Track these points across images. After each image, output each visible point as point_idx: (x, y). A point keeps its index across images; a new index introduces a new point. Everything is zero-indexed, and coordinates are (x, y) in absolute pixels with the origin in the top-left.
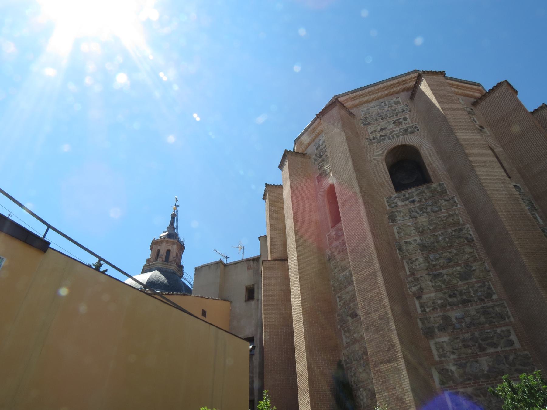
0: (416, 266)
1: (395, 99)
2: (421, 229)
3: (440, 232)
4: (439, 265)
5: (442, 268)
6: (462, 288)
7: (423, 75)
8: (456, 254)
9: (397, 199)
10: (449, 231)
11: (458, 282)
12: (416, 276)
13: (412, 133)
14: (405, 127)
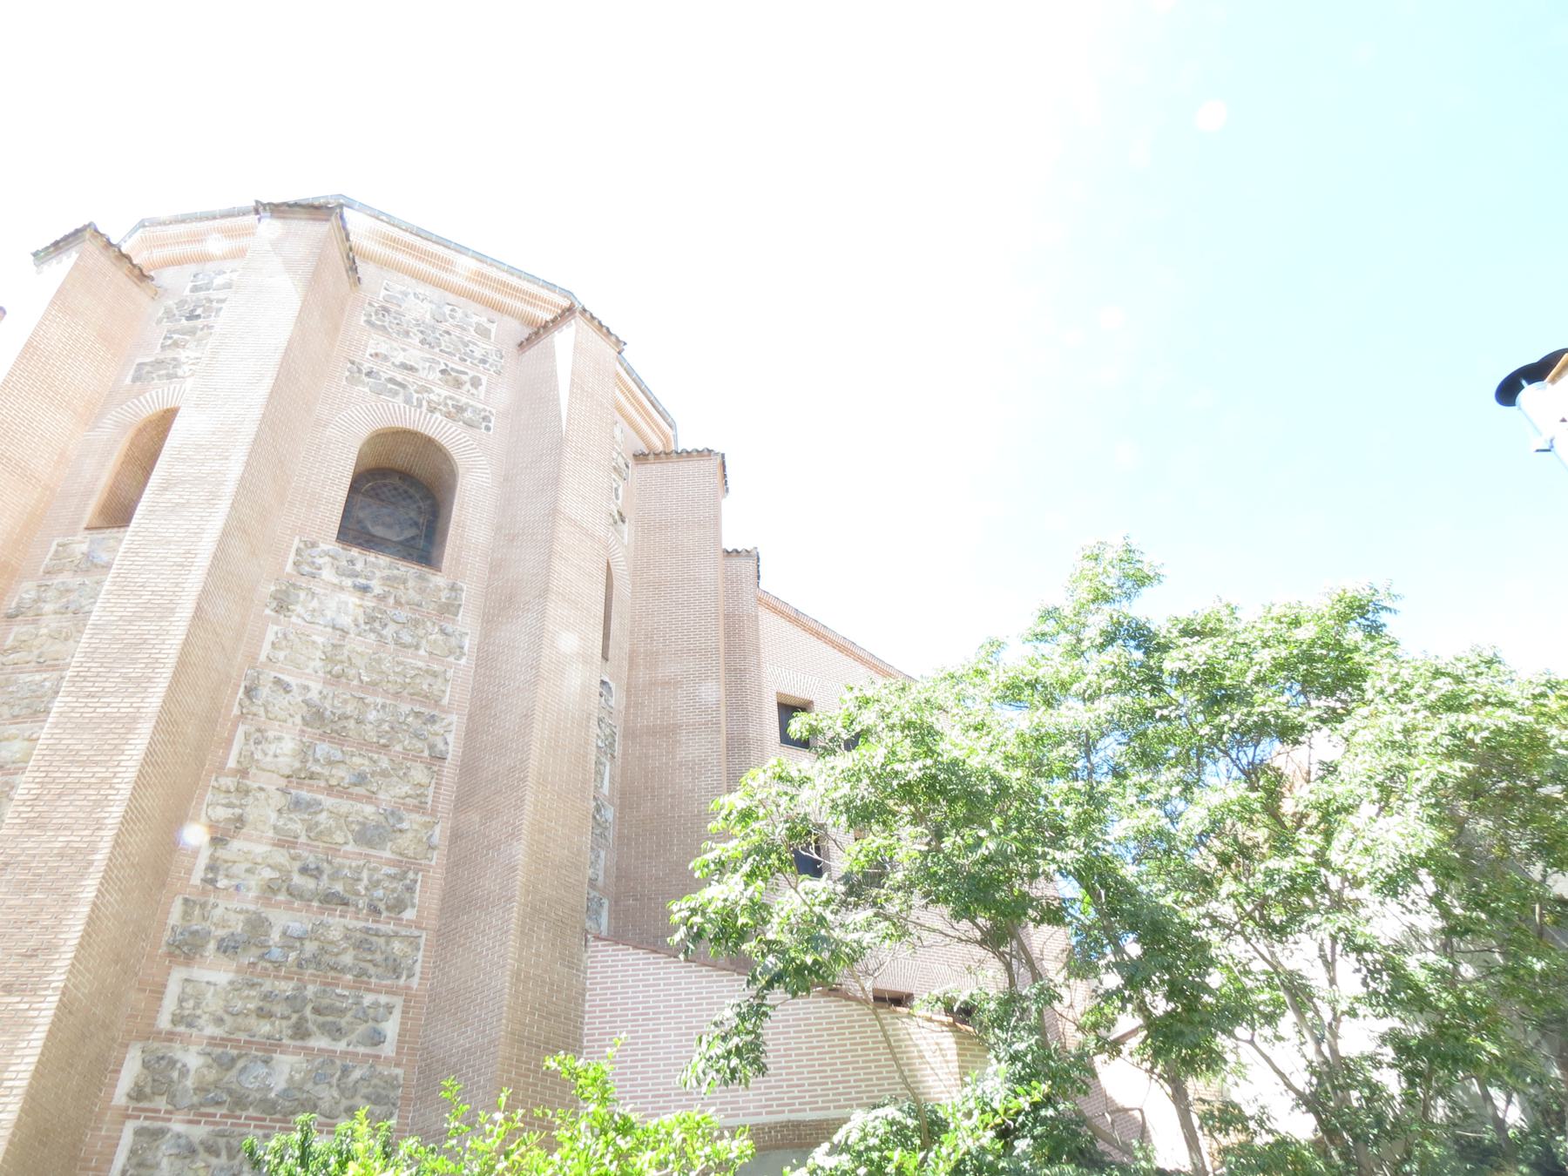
0: (266, 754)
1: (483, 320)
2: (338, 669)
3: (380, 700)
4: (327, 781)
5: (330, 789)
6: (347, 862)
7: (577, 314)
8: (384, 774)
9: (327, 559)
10: (405, 708)
11: (346, 843)
12: (248, 782)
13: (469, 424)
14: (464, 400)
